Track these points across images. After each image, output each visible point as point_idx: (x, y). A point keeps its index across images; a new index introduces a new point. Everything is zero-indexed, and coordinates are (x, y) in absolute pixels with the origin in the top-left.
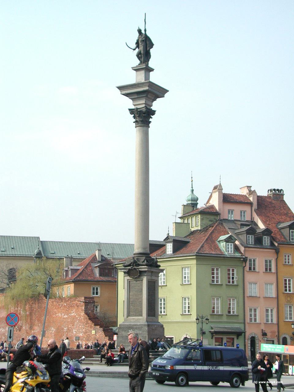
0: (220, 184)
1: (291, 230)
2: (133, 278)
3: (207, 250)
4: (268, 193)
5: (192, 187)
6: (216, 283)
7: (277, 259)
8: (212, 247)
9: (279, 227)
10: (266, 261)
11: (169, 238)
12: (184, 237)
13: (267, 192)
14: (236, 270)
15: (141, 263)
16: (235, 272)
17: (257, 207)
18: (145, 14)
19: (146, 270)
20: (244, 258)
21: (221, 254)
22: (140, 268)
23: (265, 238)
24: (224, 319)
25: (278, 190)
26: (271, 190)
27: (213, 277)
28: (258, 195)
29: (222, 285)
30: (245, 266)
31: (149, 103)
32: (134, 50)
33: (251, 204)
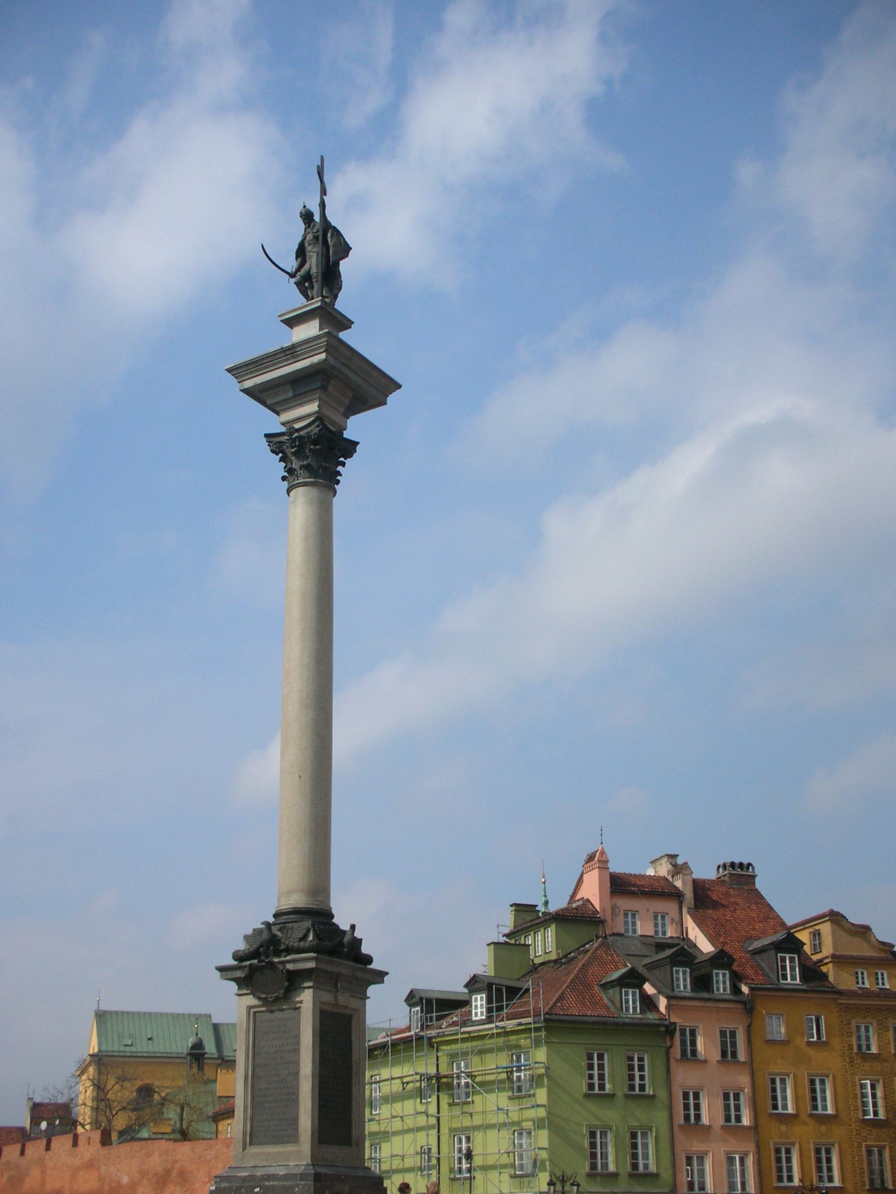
1: (779, 955)
2: (259, 998)
3: (573, 1008)
4: (718, 872)
5: (545, 896)
6: (599, 1090)
7: (749, 1026)
8: (586, 1000)
9: (750, 949)
10: (723, 1033)
11: (476, 981)
12: (518, 979)
13: (716, 872)
14: (648, 1056)
15: (296, 944)
16: (646, 1063)
17: (693, 902)
19: (311, 965)
20: (667, 1027)
21: (610, 1017)
22: (289, 962)
23: (717, 974)
24: (623, 1184)
25: (741, 865)
26: (724, 866)
27: (591, 1077)
28: (695, 876)
29: (612, 1096)
30: (671, 1047)
31: (333, 415)
33: (677, 896)
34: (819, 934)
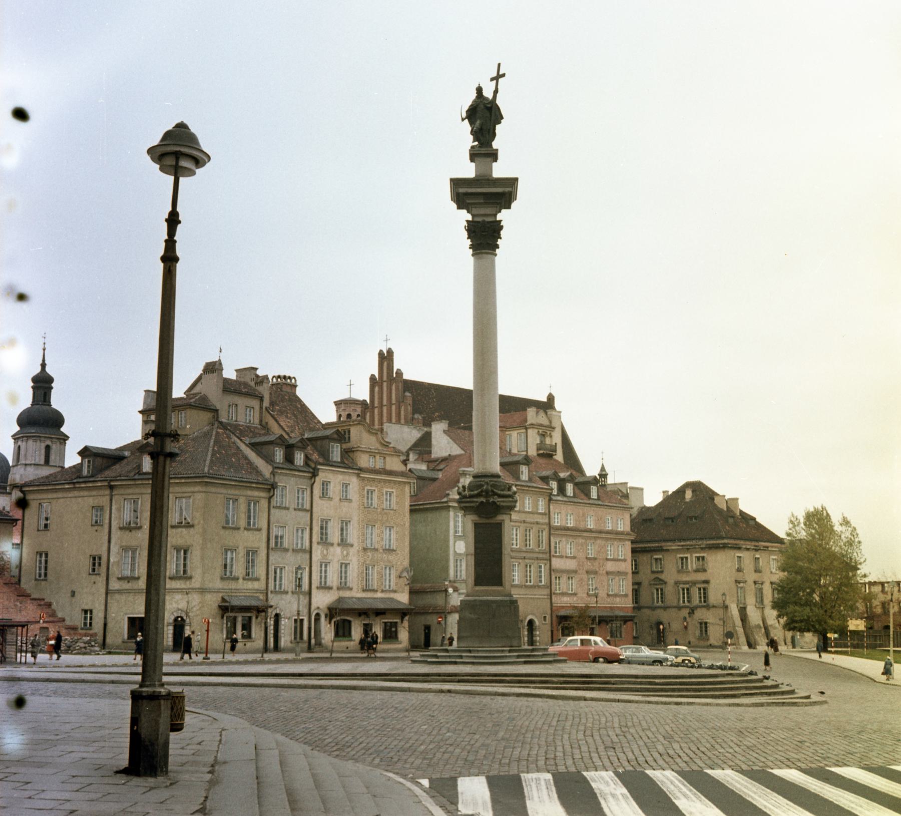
0: (220, 360)
18: (499, 65)
25: (290, 378)
26: (279, 377)
32: (463, 120)
34: (349, 432)
